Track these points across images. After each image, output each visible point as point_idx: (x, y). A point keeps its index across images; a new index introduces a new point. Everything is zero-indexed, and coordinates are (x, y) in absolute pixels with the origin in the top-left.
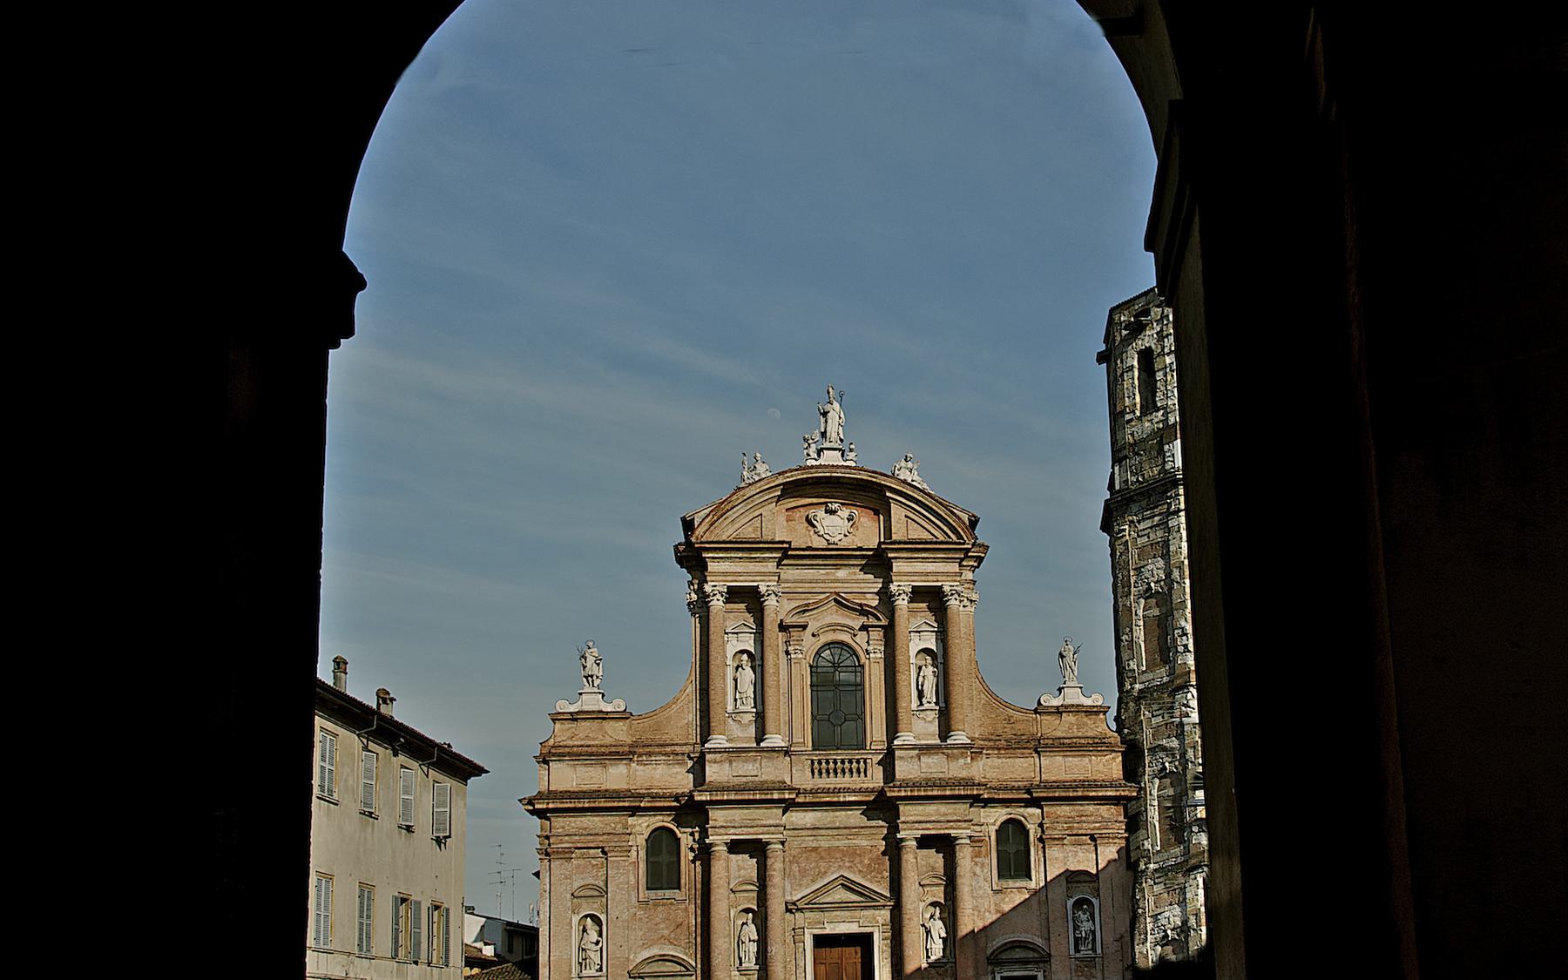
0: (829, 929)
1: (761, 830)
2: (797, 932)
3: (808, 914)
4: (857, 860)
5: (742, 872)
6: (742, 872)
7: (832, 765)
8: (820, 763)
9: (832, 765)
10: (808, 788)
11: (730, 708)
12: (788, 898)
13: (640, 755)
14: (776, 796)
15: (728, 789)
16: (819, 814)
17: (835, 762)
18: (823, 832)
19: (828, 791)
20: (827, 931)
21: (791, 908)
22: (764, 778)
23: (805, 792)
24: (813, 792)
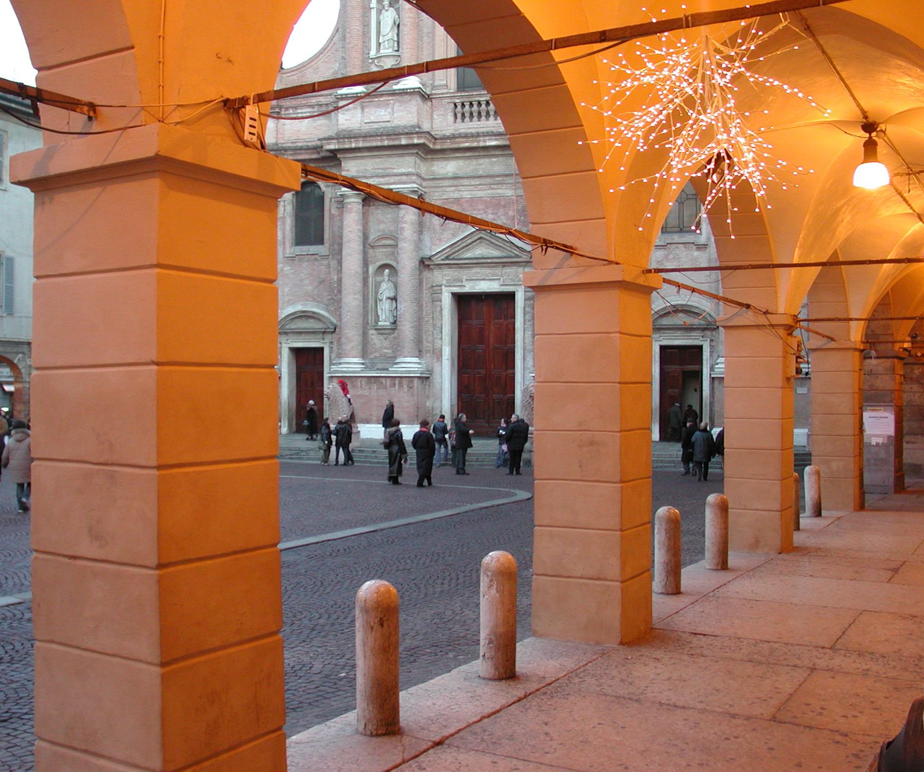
0: (469, 288)
1: (392, 180)
2: (435, 291)
3: (447, 271)
4: (501, 212)
5: (382, 226)
6: (382, 226)
7: (475, 107)
8: (463, 105)
9: (475, 107)
10: (448, 133)
11: (373, 53)
12: (428, 253)
13: (287, 109)
14: (404, 142)
15: (356, 137)
16: (461, 163)
17: (479, 104)
18: (465, 182)
19: (466, 136)
20: (467, 290)
21: (425, 264)
22: (396, 123)
23: (444, 138)
24: (453, 137)
